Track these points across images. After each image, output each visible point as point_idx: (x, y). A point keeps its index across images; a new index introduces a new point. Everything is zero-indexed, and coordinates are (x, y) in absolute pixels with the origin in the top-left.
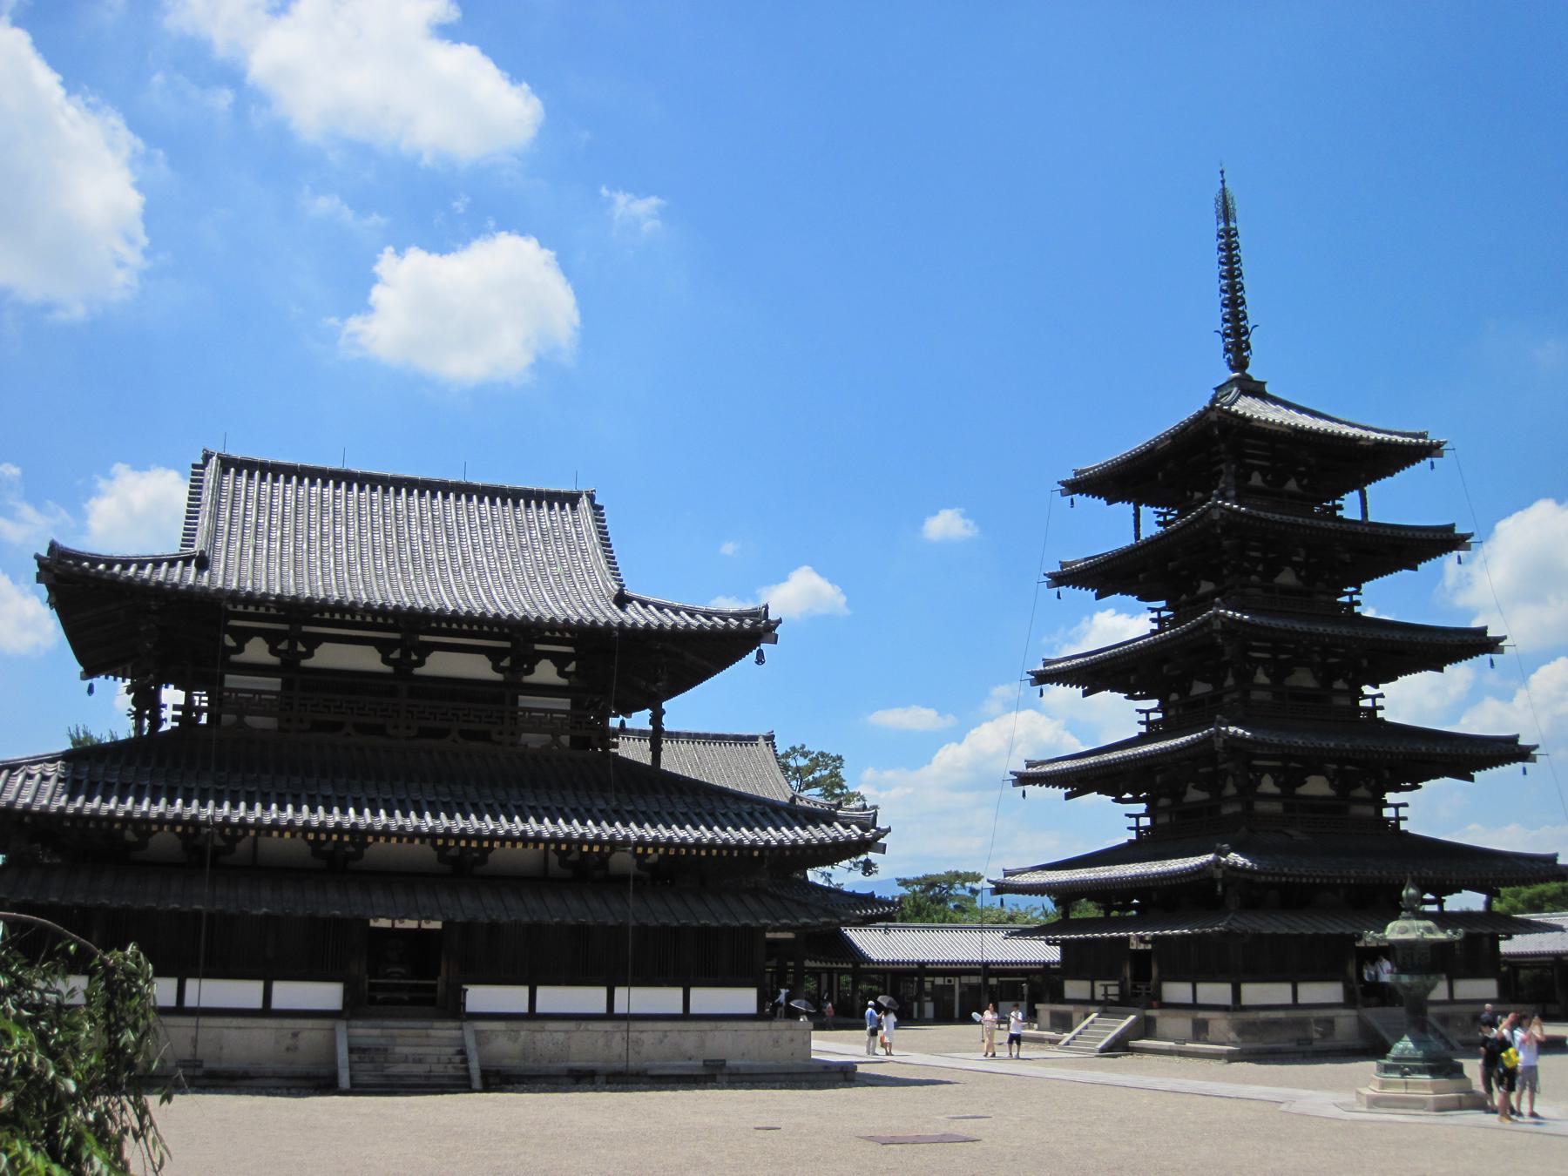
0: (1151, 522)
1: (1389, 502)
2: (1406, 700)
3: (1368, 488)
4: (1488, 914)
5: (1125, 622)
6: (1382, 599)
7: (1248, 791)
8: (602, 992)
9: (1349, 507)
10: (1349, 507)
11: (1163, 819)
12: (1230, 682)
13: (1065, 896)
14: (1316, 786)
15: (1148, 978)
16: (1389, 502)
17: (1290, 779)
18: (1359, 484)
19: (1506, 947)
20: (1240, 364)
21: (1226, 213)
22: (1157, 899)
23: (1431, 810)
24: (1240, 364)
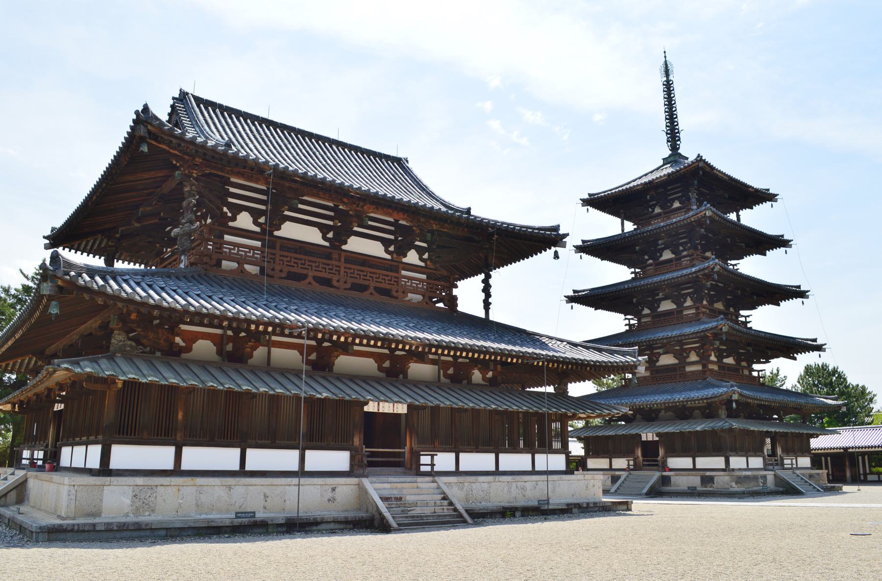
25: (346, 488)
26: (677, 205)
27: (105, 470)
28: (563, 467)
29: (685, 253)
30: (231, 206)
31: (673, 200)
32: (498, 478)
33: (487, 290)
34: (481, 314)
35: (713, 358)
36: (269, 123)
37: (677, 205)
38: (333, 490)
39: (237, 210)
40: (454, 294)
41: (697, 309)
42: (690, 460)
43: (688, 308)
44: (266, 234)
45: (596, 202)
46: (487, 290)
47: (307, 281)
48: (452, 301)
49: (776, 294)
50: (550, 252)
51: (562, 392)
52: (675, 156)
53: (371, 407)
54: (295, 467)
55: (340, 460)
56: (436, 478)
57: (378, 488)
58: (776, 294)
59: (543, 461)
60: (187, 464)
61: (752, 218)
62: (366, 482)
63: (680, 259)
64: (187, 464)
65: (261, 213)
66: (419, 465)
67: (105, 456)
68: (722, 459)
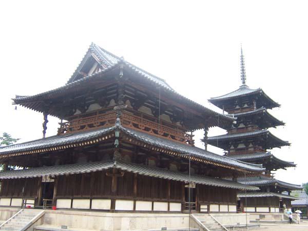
8: (150, 204)
20: (244, 83)
24: (244, 83)
26: (246, 106)
27: (72, 208)
29: (249, 126)
31: (244, 104)
32: (218, 214)
37: (246, 106)
38: (183, 219)
40: (193, 139)
41: (255, 148)
42: (254, 208)
43: (251, 148)
47: (150, 131)
52: (244, 87)
56: (210, 214)
61: (273, 112)
63: (247, 128)
67: (113, 205)
68: (268, 208)
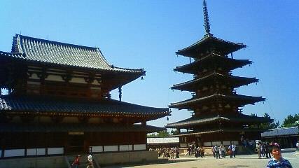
0: (193, 60)
1: (237, 55)
2: (241, 91)
3: (233, 53)
4: (258, 129)
5: (189, 77)
6: (236, 73)
7: (217, 107)
9: (229, 56)
10: (229, 56)
11: (198, 113)
12: (211, 87)
13: (179, 128)
14: (228, 106)
15: (188, 142)
16: (237, 55)
17: (224, 105)
18: (231, 52)
19: (262, 135)
20: (208, 31)
21: (205, 4)
22: (196, 128)
23: (247, 110)
24: (208, 31)
25: (59, 159)
28: (145, 148)
30: (29, 72)
33: (120, 91)
34: (119, 100)
35: (220, 106)
36: (47, 42)
39: (31, 73)
44: (42, 80)
45: (180, 53)
46: (120, 91)
48: (109, 96)
49: (246, 81)
50: (140, 78)
51: (144, 124)
53: (70, 133)
54: (44, 154)
55: (60, 150)
57: (67, 159)
58: (246, 81)
59: (137, 147)
60: (6, 155)
62: (66, 157)
64: (6, 155)
65: (40, 73)
66: (88, 150)
